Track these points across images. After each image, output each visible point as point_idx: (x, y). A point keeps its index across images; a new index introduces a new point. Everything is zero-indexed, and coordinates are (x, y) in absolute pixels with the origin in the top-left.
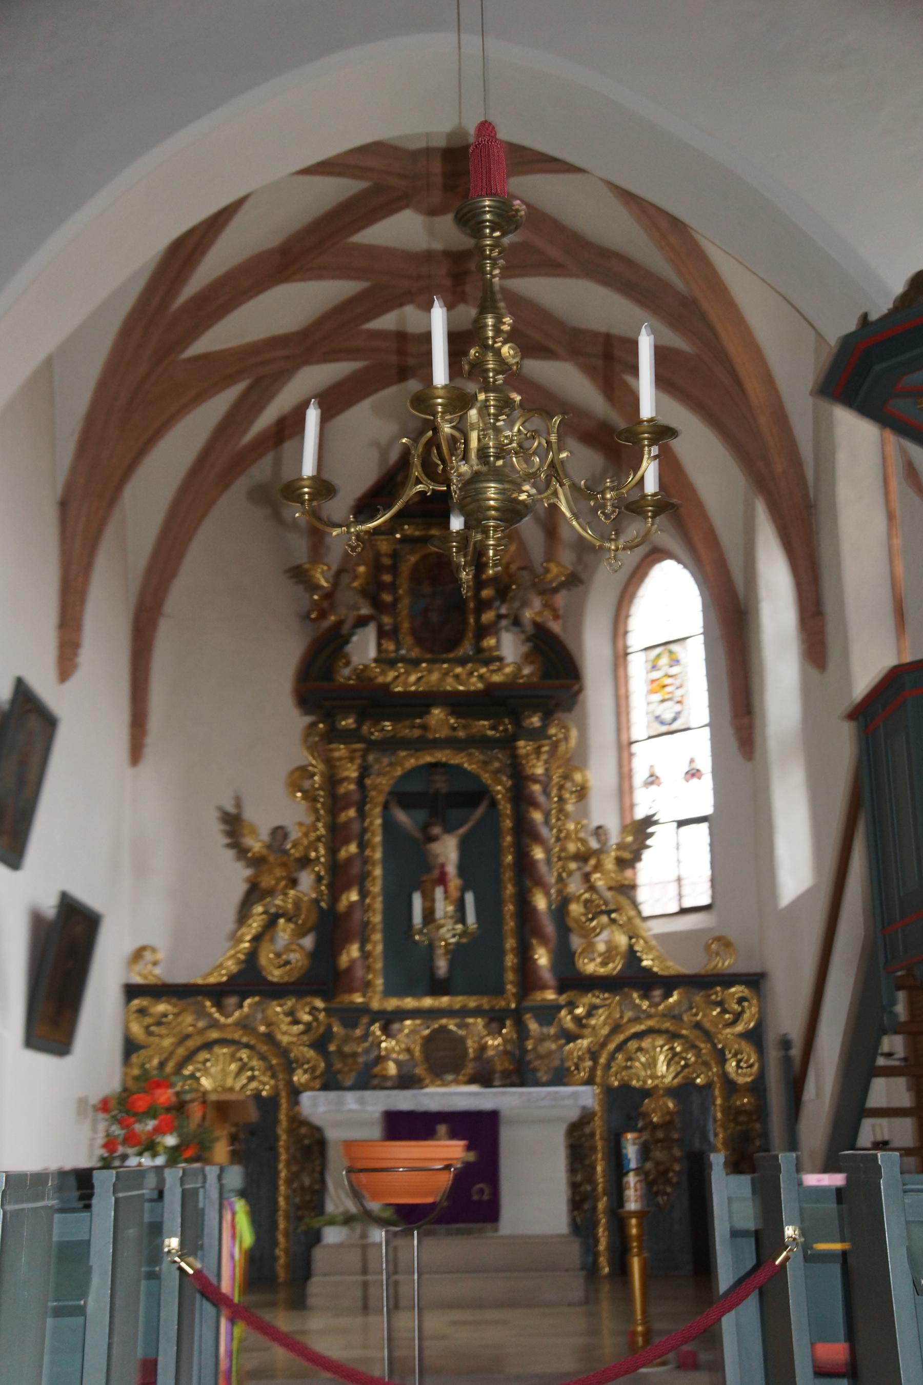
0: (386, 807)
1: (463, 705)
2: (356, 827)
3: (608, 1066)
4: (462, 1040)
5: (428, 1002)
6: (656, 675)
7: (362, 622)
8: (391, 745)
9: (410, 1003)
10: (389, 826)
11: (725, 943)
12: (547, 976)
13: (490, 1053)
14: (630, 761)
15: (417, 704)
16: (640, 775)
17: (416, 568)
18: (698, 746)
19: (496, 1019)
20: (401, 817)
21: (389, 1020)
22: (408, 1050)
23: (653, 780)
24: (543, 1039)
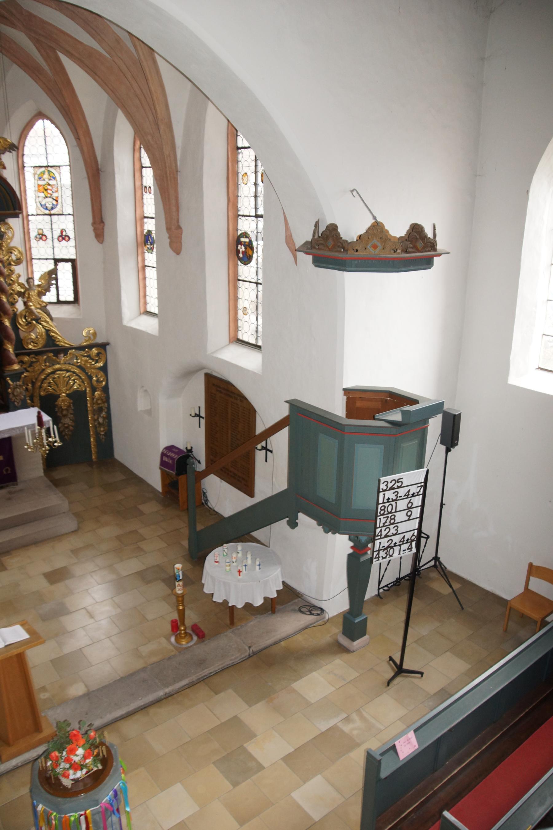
6: (41, 183)
12: (13, 357)
14: (28, 225)
16: (33, 234)
18: (67, 224)
23: (41, 236)
24: (16, 387)
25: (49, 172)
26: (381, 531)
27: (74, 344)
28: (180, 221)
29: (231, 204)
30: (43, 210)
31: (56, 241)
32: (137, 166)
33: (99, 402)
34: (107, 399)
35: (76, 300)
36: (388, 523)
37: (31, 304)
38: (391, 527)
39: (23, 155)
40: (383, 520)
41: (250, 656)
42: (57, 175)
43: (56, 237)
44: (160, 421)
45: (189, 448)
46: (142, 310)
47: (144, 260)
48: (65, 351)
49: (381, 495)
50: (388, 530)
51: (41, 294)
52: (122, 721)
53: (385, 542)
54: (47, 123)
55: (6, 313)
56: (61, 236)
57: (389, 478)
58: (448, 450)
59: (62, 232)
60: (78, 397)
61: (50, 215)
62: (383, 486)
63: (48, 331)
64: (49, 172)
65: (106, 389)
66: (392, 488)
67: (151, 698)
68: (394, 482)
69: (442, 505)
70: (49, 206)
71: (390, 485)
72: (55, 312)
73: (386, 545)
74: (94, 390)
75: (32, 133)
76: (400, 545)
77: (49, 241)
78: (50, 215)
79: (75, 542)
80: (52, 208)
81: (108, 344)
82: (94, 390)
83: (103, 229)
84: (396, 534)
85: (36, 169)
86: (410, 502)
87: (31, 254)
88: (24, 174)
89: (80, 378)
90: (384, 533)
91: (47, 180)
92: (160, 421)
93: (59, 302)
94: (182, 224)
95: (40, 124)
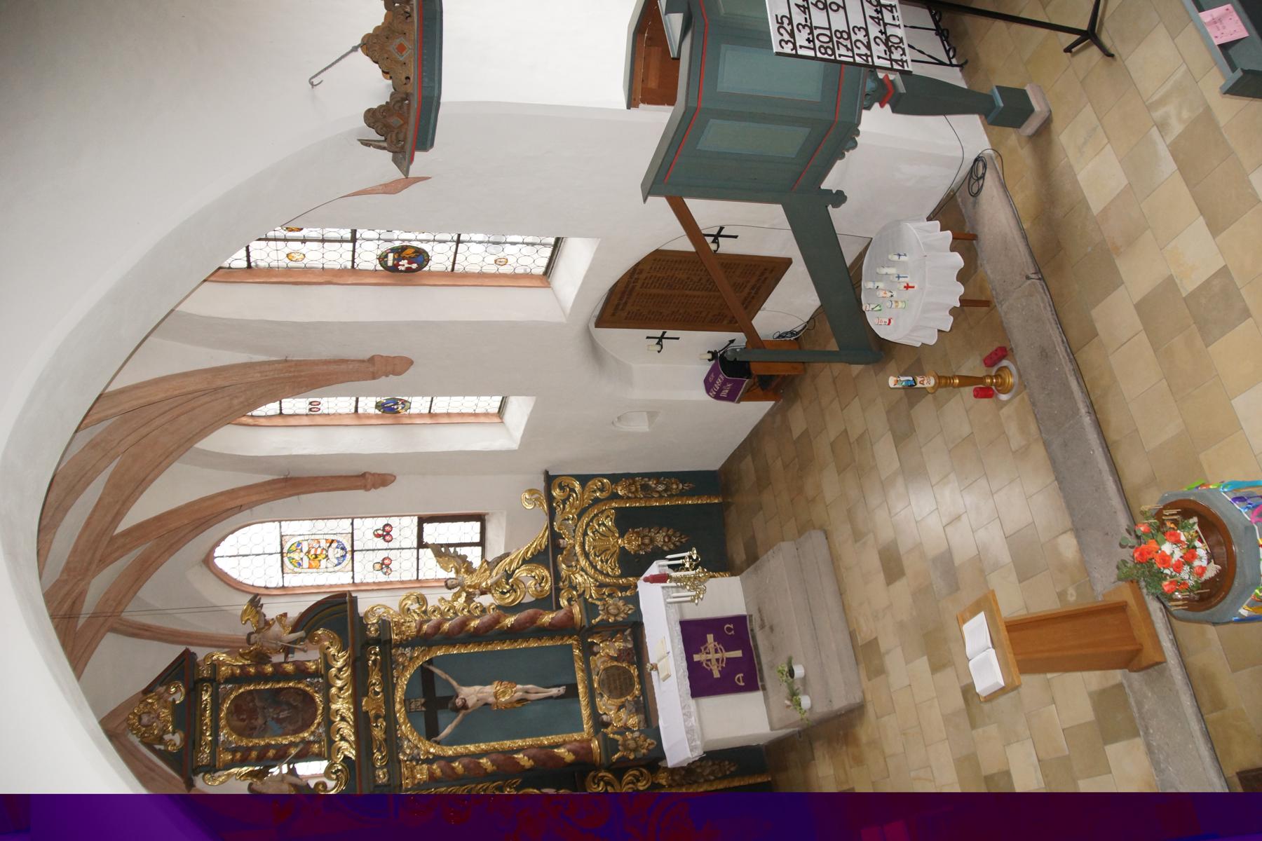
0: (438, 743)
1: (359, 688)
2: (466, 760)
3: (607, 575)
4: (606, 670)
5: (583, 700)
6: (306, 563)
7: (292, 772)
8: (393, 742)
9: (585, 713)
10: (450, 741)
12: (561, 613)
13: (613, 653)
14: (368, 584)
15: (362, 723)
16: (381, 577)
17: (241, 733)
18: (366, 528)
19: (588, 651)
20: (446, 732)
21: (599, 724)
22: (619, 708)
23: (385, 565)
25: (289, 552)
26: (859, 55)
27: (546, 523)
28: (361, 358)
29: (335, 280)
30: (344, 564)
31: (391, 545)
32: (280, 421)
33: (633, 489)
34: (630, 477)
35: (480, 518)
37: (484, 585)
38: (854, 38)
39: (266, 588)
40: (843, 51)
41: (1042, 279)
42: (295, 540)
43: (384, 545)
44: (666, 399)
45: (710, 356)
46: (497, 420)
47: (421, 415)
48: (554, 537)
49: (801, 52)
50: (859, 44)
51: (470, 570)
52: (1124, 482)
53: (879, 50)
54: (218, 552)
55: (497, 621)
56: (384, 537)
59: (378, 536)
60: (626, 520)
61: (353, 551)
62: (788, 49)
63: (525, 562)
64: (289, 552)
65: (615, 478)
66: (792, 34)
67: (1092, 436)
68: (782, 31)
70: (341, 553)
71: (787, 37)
72: (496, 547)
73: (882, 47)
74: (615, 496)
75: (234, 574)
76: (885, 24)
77: (392, 554)
78: (353, 551)
79: (842, 534)
80: (343, 549)
81: (547, 473)
82: (615, 496)
83: (373, 475)
84: (866, 30)
85: (286, 570)
86: (816, 5)
87: (410, 581)
88: (294, 588)
89: (596, 515)
90: (864, 51)
91: (302, 555)
92: (666, 399)
93: (482, 543)
94: (367, 356)
95: (219, 563)
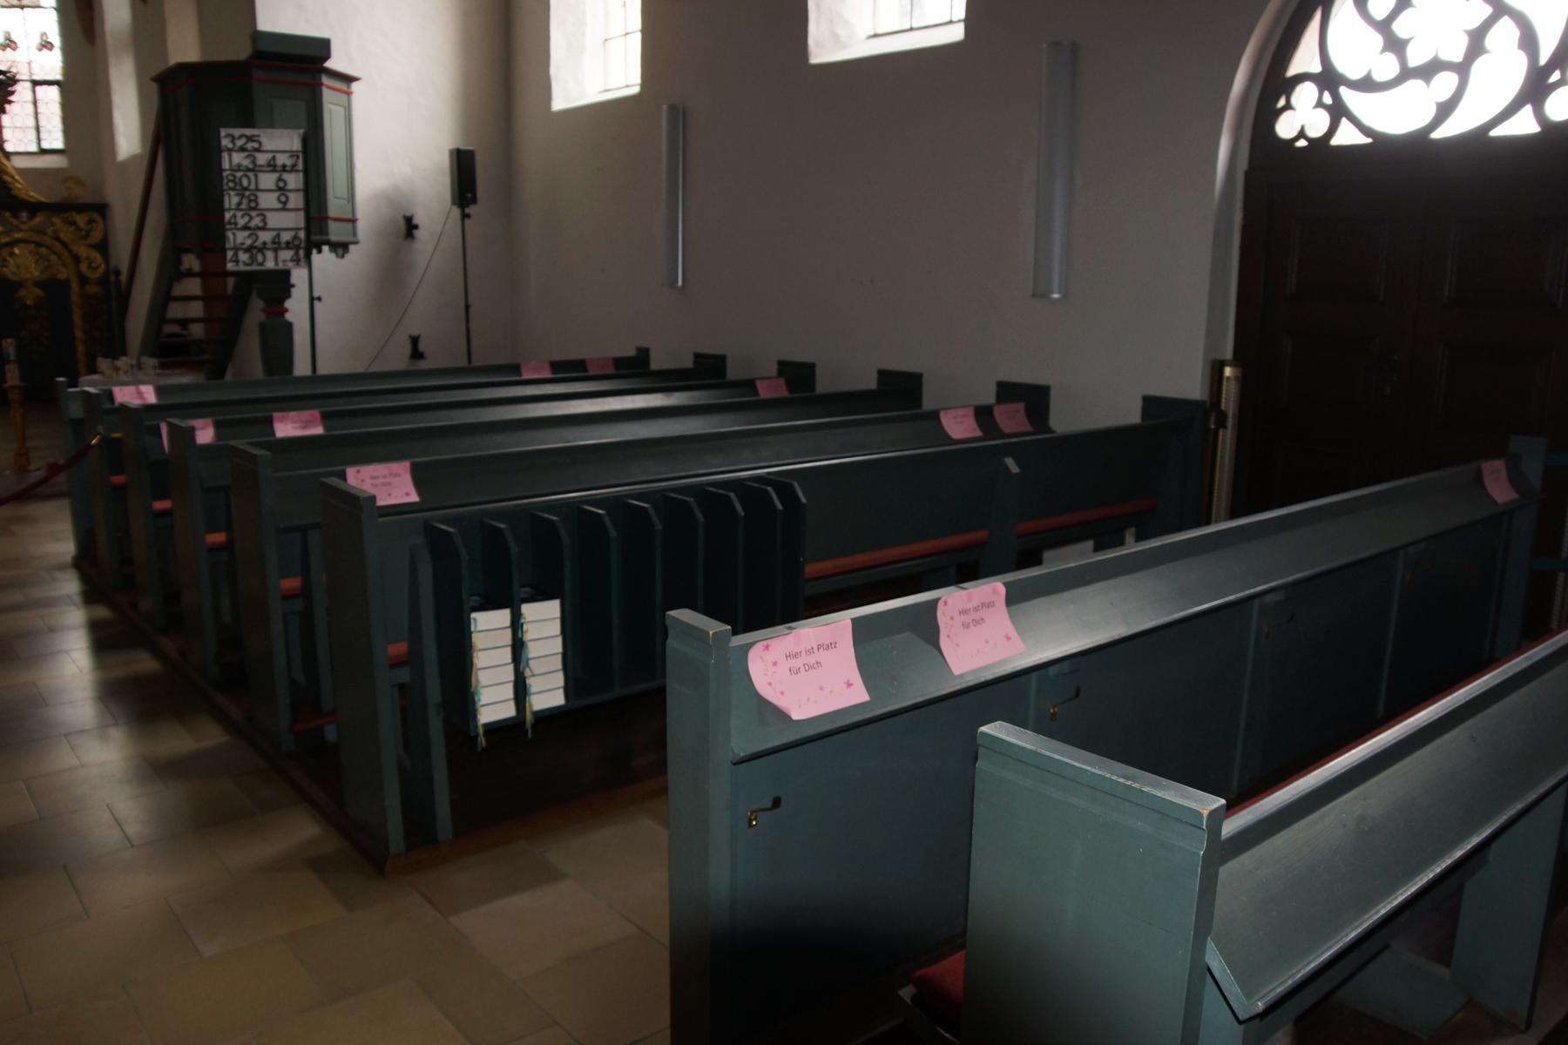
11: (78, 182)
26: (234, 216)
36: (243, 206)
38: (254, 213)
40: (235, 200)
49: (225, 155)
57: (237, 132)
58: (465, 216)
62: (225, 142)
66: (242, 149)
69: (467, 307)
71: (239, 143)
73: (249, 242)
76: (276, 251)
84: (264, 228)
86: (280, 179)
90: (241, 222)
93: (43, 152)
